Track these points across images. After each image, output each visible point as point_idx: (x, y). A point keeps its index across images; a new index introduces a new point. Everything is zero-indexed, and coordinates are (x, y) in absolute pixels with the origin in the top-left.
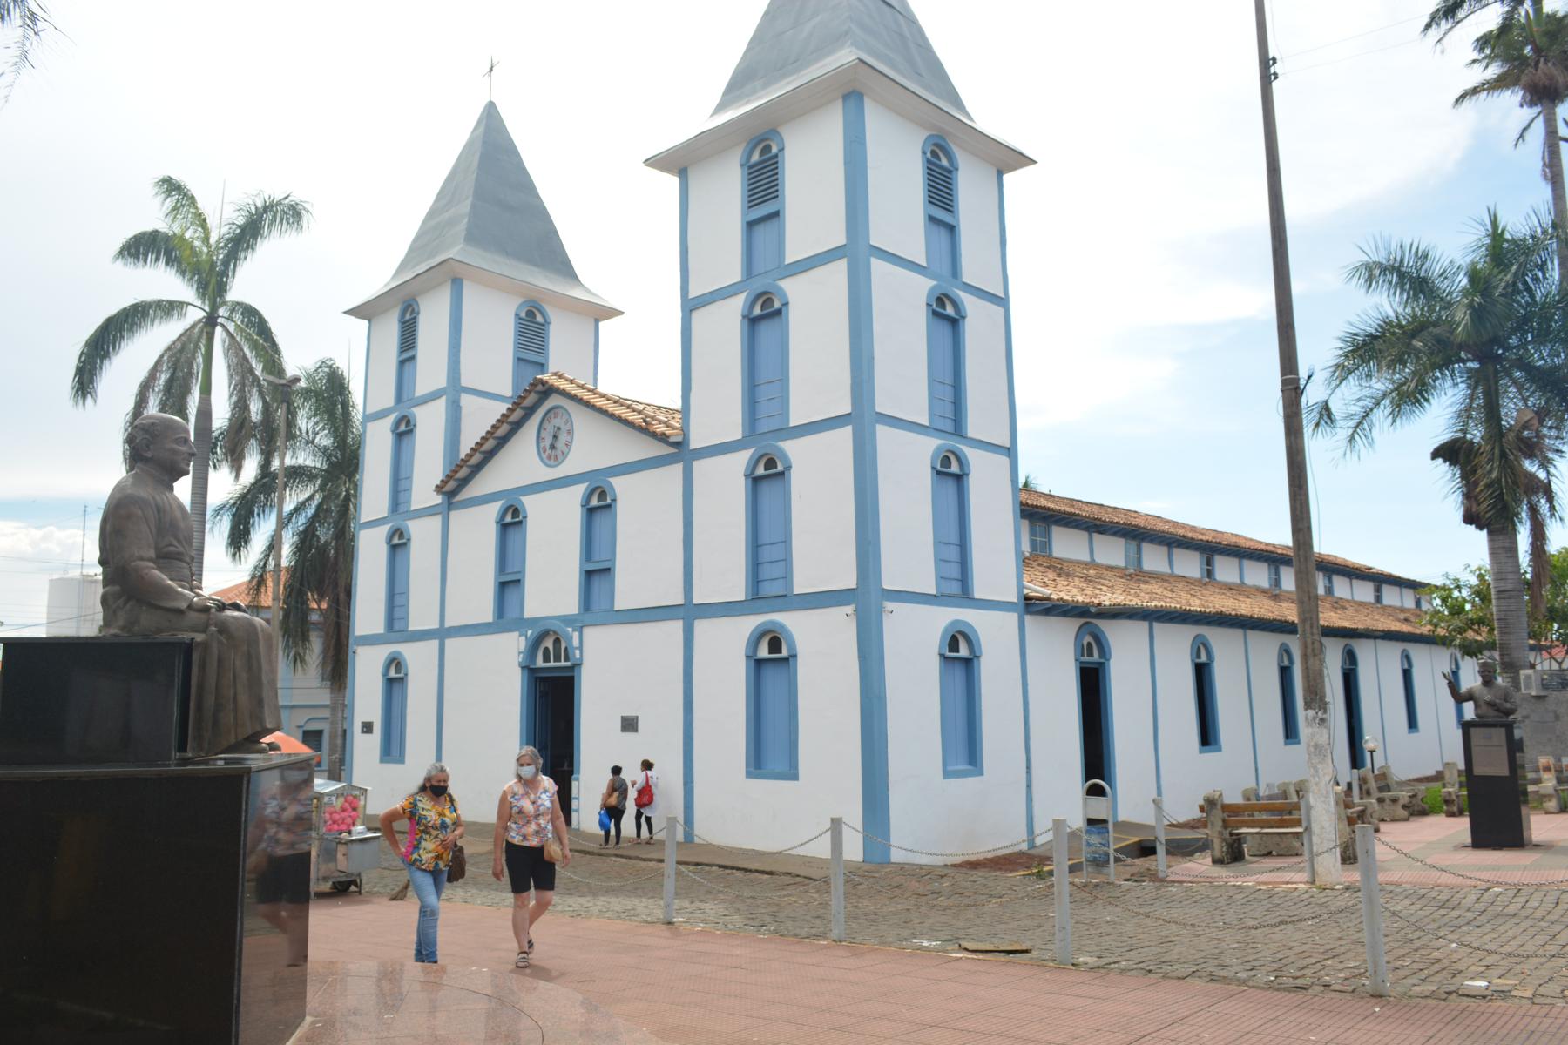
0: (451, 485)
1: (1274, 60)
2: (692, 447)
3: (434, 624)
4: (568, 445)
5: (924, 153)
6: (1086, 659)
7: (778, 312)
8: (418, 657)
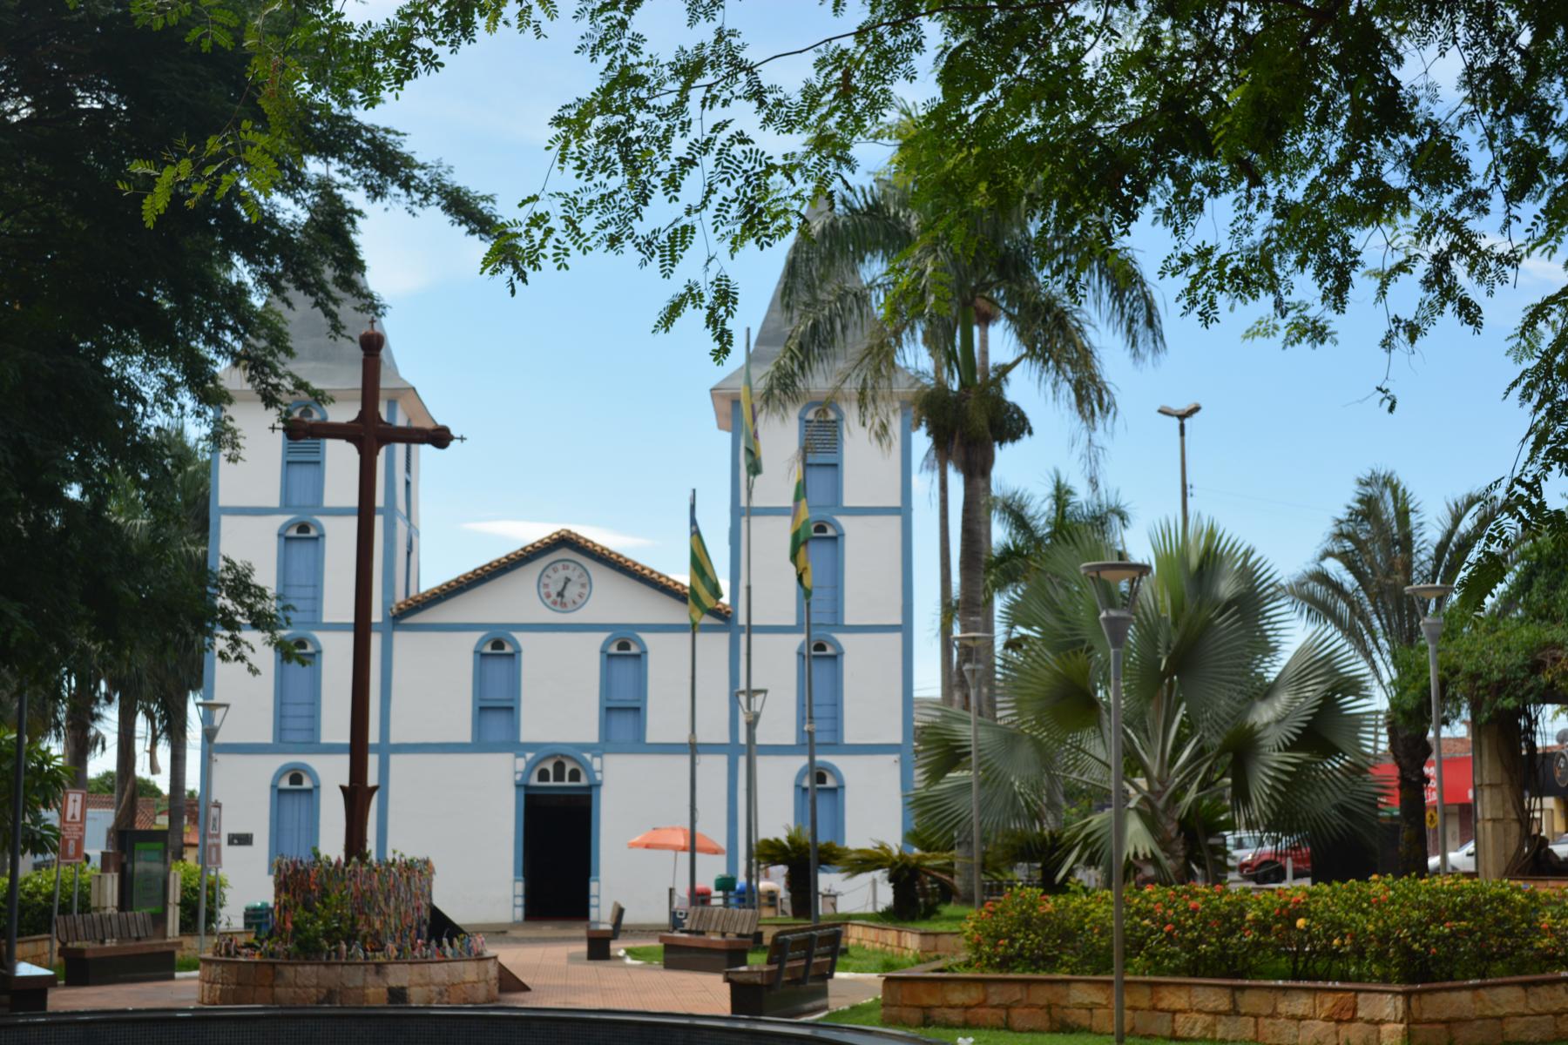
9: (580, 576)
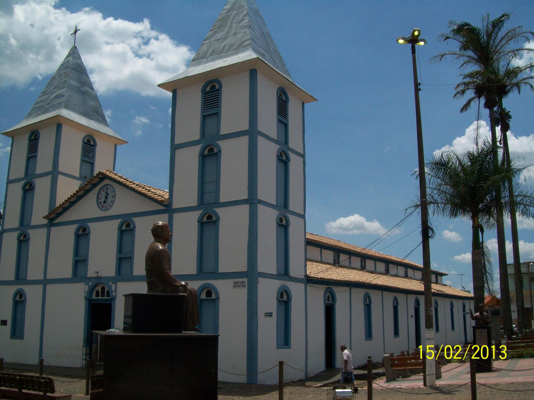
0: (53, 215)
1: (420, 84)
2: (173, 207)
3: (41, 277)
4: (113, 202)
5: (277, 94)
6: (327, 302)
7: (216, 154)
8: (33, 294)
9: (112, 192)
